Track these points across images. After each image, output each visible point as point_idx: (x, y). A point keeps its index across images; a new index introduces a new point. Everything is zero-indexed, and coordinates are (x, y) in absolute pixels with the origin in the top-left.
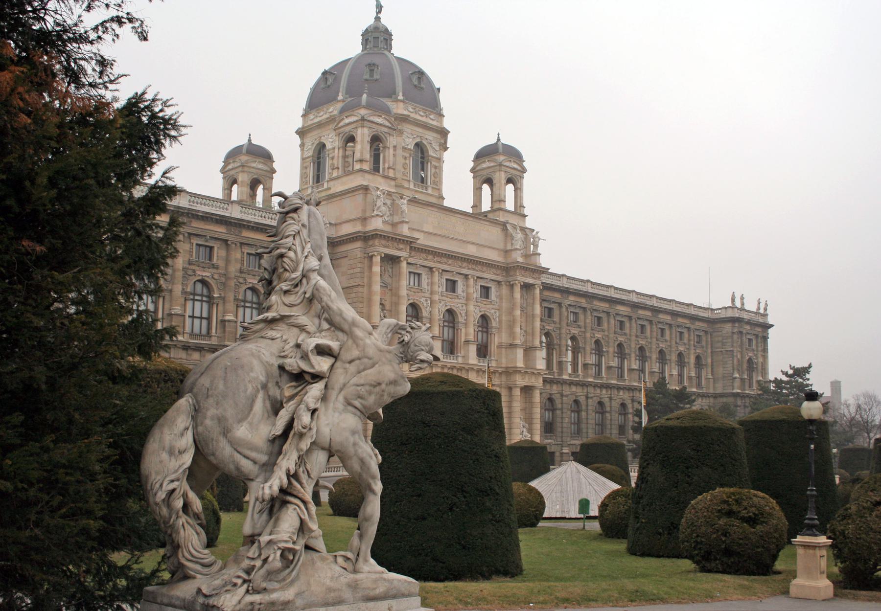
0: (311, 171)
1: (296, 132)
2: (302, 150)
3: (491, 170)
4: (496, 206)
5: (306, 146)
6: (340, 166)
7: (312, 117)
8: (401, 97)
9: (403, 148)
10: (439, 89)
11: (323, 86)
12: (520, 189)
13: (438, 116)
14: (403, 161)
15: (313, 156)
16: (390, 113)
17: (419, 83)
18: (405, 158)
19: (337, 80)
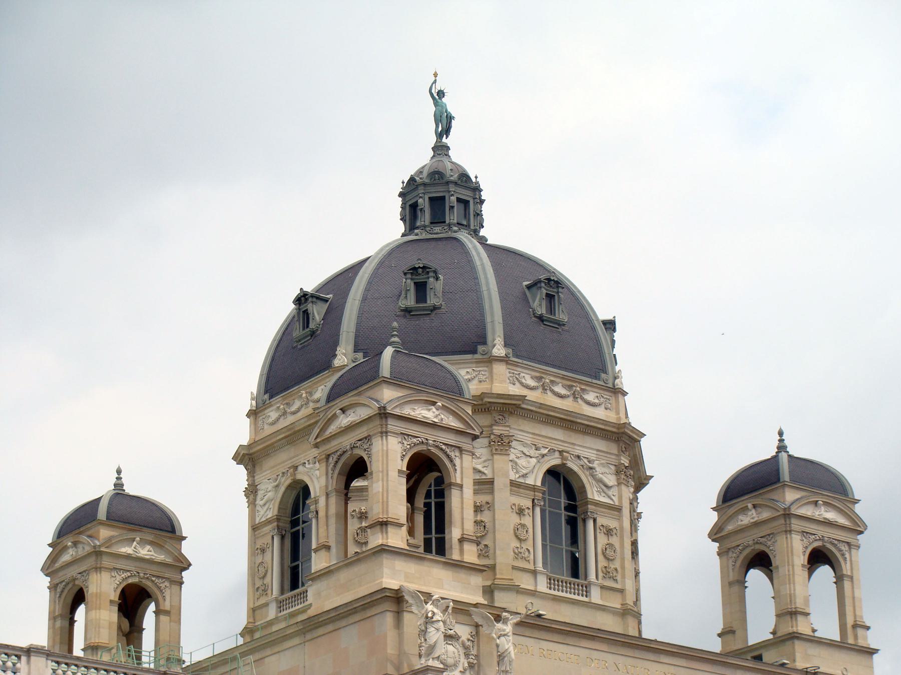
0: (274, 559)
1: (234, 458)
2: (252, 504)
3: (765, 530)
4: (787, 628)
5: (260, 494)
6: (332, 543)
7: (273, 415)
8: (499, 350)
9: (513, 484)
10: (610, 325)
11: (298, 332)
12: (851, 578)
13: (607, 395)
14: (515, 519)
15: (278, 519)
16: (461, 393)
17: (551, 309)
18: (520, 512)
19: (334, 314)
